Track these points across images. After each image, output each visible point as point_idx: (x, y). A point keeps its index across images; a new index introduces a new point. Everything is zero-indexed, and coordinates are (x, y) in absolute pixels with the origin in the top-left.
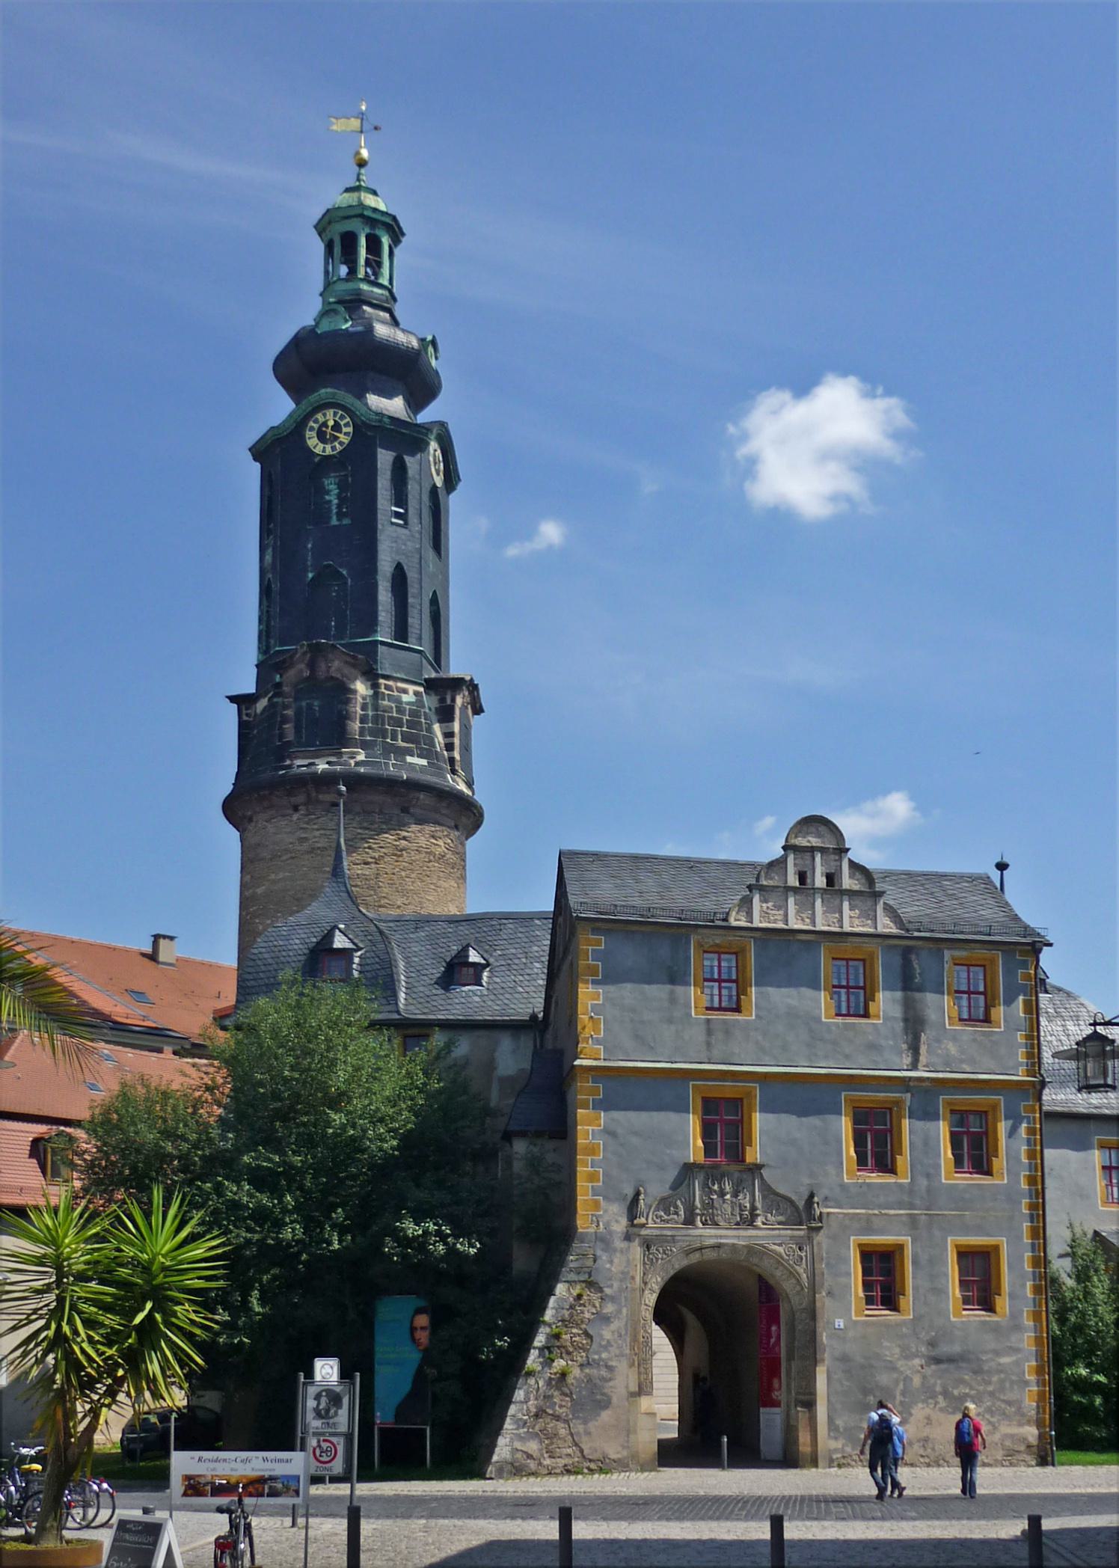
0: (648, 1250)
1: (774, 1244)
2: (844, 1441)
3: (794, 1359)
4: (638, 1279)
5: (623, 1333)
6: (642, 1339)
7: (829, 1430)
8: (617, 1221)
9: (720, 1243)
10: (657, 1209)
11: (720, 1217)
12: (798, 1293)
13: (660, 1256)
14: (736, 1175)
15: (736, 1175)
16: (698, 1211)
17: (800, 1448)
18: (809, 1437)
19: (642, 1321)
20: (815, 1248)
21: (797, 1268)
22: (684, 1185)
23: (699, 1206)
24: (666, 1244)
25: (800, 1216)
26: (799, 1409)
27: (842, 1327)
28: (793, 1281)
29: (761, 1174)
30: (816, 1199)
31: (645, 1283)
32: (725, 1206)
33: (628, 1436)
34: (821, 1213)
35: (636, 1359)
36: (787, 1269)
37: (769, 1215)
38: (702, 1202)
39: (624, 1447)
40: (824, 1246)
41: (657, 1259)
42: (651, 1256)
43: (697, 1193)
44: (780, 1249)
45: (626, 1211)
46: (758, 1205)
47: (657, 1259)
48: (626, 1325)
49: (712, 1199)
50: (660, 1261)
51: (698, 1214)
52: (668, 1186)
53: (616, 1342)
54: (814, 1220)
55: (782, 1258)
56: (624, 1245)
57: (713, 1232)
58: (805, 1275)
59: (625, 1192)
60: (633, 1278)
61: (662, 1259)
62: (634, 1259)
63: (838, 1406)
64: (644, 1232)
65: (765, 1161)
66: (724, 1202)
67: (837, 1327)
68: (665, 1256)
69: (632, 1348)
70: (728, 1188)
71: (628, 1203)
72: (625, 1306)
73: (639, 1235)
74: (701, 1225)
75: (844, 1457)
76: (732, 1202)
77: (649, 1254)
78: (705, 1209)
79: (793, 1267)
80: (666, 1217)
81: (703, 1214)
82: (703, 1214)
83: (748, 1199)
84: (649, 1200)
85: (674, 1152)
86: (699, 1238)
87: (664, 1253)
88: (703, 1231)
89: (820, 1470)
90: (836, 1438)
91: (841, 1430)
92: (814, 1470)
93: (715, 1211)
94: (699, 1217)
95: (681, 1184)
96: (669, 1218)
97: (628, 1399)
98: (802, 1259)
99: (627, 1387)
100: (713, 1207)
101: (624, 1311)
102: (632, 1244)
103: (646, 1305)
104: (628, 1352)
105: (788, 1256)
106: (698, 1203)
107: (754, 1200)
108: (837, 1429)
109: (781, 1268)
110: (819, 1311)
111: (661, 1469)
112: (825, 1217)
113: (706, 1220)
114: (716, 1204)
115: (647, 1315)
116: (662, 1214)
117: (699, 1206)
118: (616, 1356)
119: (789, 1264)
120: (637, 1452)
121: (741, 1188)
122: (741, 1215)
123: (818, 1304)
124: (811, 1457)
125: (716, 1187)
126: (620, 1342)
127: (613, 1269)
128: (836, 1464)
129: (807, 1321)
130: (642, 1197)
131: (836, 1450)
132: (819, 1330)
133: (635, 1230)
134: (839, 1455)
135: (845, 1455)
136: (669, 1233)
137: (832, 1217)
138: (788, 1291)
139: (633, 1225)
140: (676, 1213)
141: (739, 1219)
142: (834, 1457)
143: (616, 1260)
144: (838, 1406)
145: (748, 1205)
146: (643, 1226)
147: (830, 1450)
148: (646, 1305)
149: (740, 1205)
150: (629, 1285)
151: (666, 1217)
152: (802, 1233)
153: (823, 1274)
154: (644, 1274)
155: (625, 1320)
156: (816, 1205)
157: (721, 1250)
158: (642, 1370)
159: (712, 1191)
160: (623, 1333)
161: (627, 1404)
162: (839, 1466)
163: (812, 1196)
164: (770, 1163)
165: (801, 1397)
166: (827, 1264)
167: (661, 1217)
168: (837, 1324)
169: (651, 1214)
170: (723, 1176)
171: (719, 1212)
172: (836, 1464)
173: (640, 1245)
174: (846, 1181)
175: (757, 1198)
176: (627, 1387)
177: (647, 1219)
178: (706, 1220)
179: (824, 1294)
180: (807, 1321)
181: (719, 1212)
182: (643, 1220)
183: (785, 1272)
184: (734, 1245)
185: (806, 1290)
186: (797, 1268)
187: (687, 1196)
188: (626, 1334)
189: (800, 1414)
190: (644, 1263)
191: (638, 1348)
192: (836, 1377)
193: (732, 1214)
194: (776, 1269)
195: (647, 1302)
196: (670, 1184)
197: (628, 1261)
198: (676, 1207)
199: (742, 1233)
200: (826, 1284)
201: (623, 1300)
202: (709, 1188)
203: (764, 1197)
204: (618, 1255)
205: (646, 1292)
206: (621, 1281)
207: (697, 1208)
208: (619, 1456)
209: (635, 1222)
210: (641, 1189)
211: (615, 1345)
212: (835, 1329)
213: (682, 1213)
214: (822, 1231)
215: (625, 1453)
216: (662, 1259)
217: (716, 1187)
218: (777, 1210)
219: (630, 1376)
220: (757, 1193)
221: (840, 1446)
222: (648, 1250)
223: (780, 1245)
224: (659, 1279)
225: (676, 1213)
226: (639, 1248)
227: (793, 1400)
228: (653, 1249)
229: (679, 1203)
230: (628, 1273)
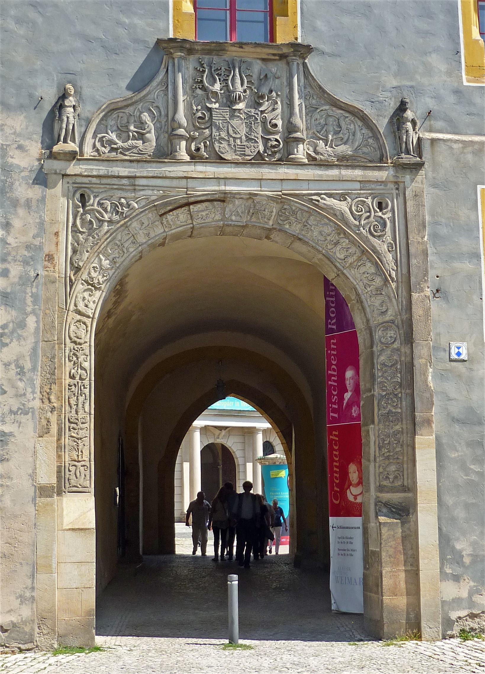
0: (84, 206)
1: (330, 196)
2: (472, 584)
3: (373, 422)
4: (61, 260)
5: (28, 365)
6: (68, 381)
7: (443, 560)
8: (20, 147)
9: (225, 193)
10: (102, 127)
11: (224, 144)
12: (379, 291)
13: (106, 217)
14: (257, 67)
15: (257, 67)
16: (182, 131)
17: (386, 599)
18: (402, 575)
19: (70, 345)
20: (410, 204)
21: (376, 242)
22: (154, 83)
23: (184, 122)
24: (119, 194)
25: (381, 147)
26: (382, 519)
27: (464, 356)
28: (370, 268)
29: (305, 65)
30: (409, 114)
31: (77, 269)
32: (235, 122)
33: (33, 576)
34: (419, 139)
35: (54, 418)
36: (353, 242)
37: (321, 143)
38: (191, 114)
39: (22, 599)
40: (427, 200)
41: (101, 222)
42: (89, 217)
43: (181, 98)
44: (343, 206)
45: (40, 130)
46: (299, 121)
47: (101, 222)
48: (34, 350)
49: (210, 110)
50: (106, 227)
51: (181, 137)
52: (124, 84)
53: (13, 386)
54: (408, 152)
55: (347, 224)
56: (36, 192)
57: (210, 170)
58: (390, 257)
59: (38, 93)
60: (50, 258)
61: (110, 222)
62: (53, 222)
63: (460, 513)
64: (73, 168)
65: (310, 41)
66: (232, 116)
67: (454, 356)
68: (115, 217)
69: (46, 397)
70: (239, 88)
71: (45, 115)
72: (34, 312)
73: (64, 175)
74: (187, 158)
75: (473, 616)
76: (249, 117)
77: (85, 213)
78: (197, 129)
79: (366, 241)
80: (120, 143)
81: (193, 139)
82: (193, 139)
83: (279, 111)
84: (86, 110)
85: (137, 21)
86: (183, 182)
87: (115, 207)
88: (191, 168)
89: (424, 646)
90: (457, 578)
91: (467, 560)
92: (411, 644)
93: (215, 133)
94: (183, 143)
95: (152, 79)
96: (125, 145)
97: (34, 499)
98: (384, 225)
99: (33, 476)
100: (211, 124)
101: (31, 321)
102: (49, 192)
103: (79, 313)
104: (37, 403)
105: (358, 218)
106: (181, 116)
107: (292, 113)
108: (458, 558)
109: (345, 242)
110: (418, 328)
111: (99, 640)
112: (426, 148)
113: (198, 149)
114: (217, 119)
115: (82, 333)
116: (113, 136)
117: (184, 122)
118: (11, 412)
119: (359, 235)
120: (52, 611)
121: (265, 90)
122: (266, 141)
123: (417, 311)
124: (408, 619)
125: (217, 87)
126: (21, 385)
127: (10, 240)
128: (456, 631)
129: (396, 345)
130: (71, 101)
131: (457, 602)
132: (418, 362)
133: (57, 165)
134: (463, 613)
135: (475, 612)
136: (124, 171)
137: (443, 147)
138: (360, 288)
139: (52, 156)
140: (141, 136)
141: (261, 148)
142: (454, 615)
143: (17, 223)
144: (460, 513)
145: (279, 123)
146: (72, 156)
147: (443, 602)
148: (79, 313)
149: (264, 122)
150: (41, 272)
151: (120, 143)
152: (382, 175)
153: (425, 253)
154: (75, 251)
155: (31, 340)
156: (409, 125)
157: (230, 207)
158: (66, 441)
159: (209, 94)
160: (28, 365)
161: (31, 509)
162: (465, 635)
163: (402, 107)
164: (321, 46)
165: (386, 496)
166: (434, 236)
167: (111, 142)
168: (454, 351)
169: (89, 136)
170: (231, 66)
171: (223, 135)
172: (456, 631)
173: (66, 195)
174: (465, 83)
175: (297, 110)
176: (33, 476)
177: (81, 146)
178: (198, 149)
179: (428, 292)
180: (396, 345)
181: (223, 135)
182: (72, 146)
183: (353, 250)
184: (252, 196)
185: (394, 285)
186: (376, 242)
187: (160, 103)
188: (34, 369)
189: (384, 530)
190: (75, 231)
191: (58, 398)
192: (453, 455)
193: (249, 139)
194: (337, 243)
195: (81, 307)
196: (128, 81)
197: (41, 224)
198: (141, 124)
199: (267, 172)
200: (432, 273)
201: (29, 300)
202: (204, 88)
203: (311, 110)
204: (21, 211)
205: (79, 287)
206: (25, 263)
207: (180, 126)
208: (14, 618)
209: (56, 149)
210: (69, 86)
211: (11, 392)
212: (451, 360)
213: (152, 136)
214: (422, 172)
215: (26, 612)
216: (110, 222)
217: (217, 87)
218: (336, 133)
219: (40, 451)
220: (297, 101)
221: (465, 594)
222: (84, 206)
223: (342, 197)
224: (106, 263)
225: (141, 136)
226: (64, 201)
227: (372, 502)
228: (93, 202)
229: (146, 117)
230: (40, 248)
